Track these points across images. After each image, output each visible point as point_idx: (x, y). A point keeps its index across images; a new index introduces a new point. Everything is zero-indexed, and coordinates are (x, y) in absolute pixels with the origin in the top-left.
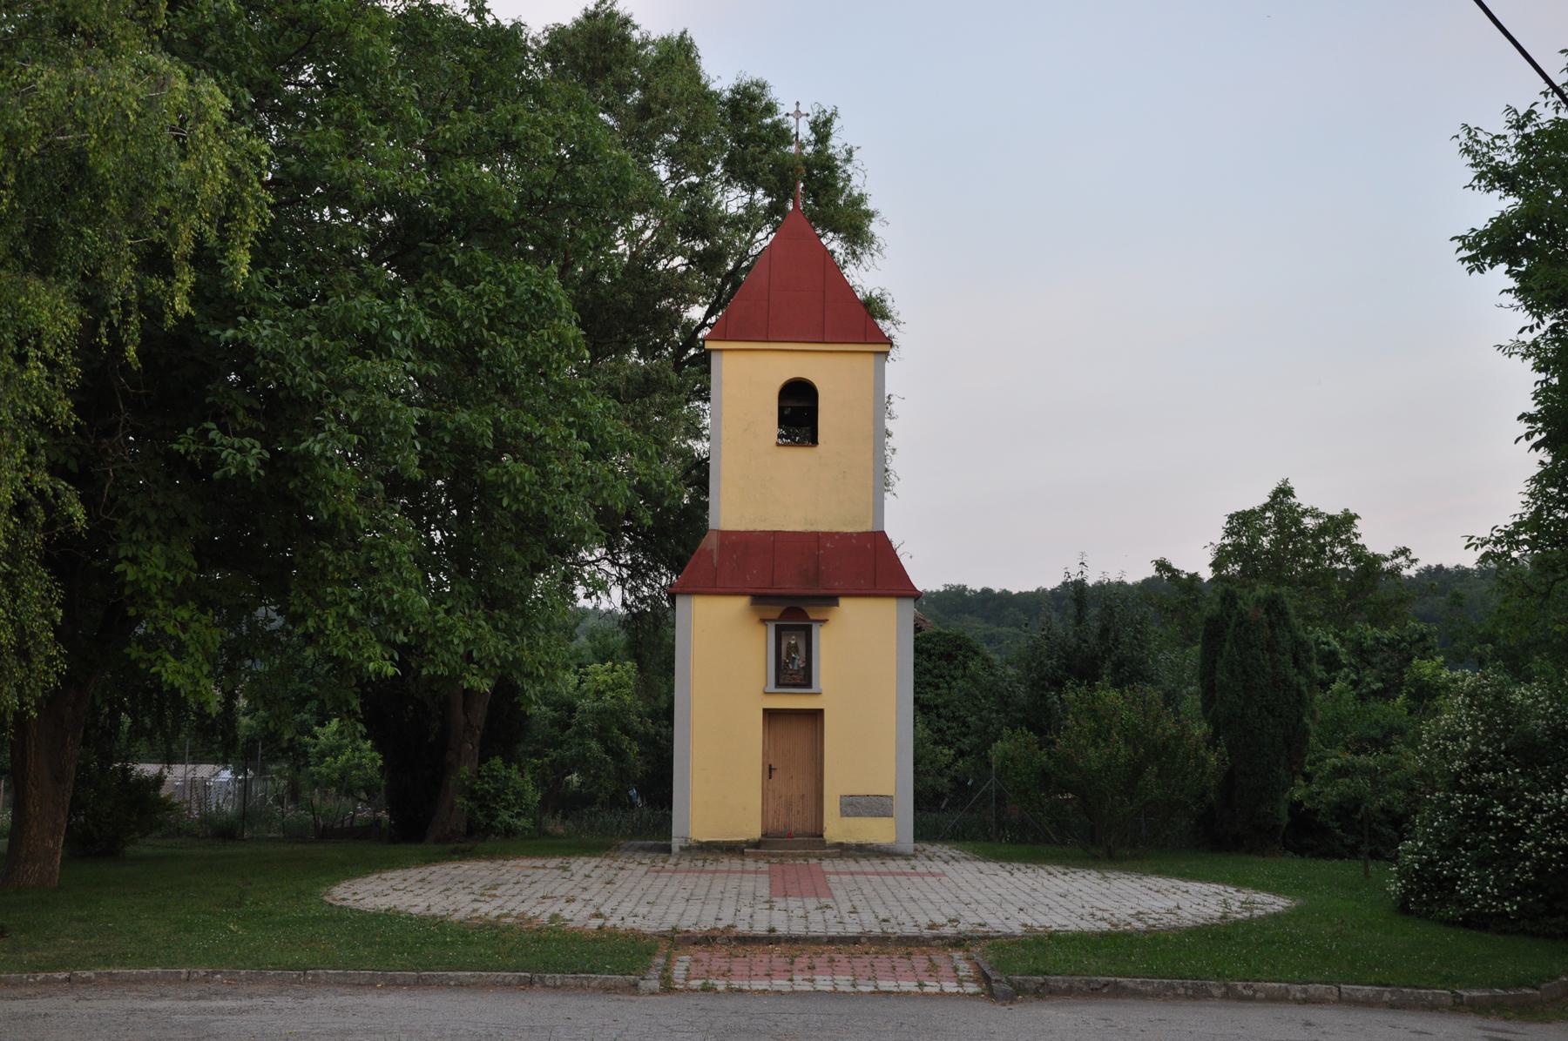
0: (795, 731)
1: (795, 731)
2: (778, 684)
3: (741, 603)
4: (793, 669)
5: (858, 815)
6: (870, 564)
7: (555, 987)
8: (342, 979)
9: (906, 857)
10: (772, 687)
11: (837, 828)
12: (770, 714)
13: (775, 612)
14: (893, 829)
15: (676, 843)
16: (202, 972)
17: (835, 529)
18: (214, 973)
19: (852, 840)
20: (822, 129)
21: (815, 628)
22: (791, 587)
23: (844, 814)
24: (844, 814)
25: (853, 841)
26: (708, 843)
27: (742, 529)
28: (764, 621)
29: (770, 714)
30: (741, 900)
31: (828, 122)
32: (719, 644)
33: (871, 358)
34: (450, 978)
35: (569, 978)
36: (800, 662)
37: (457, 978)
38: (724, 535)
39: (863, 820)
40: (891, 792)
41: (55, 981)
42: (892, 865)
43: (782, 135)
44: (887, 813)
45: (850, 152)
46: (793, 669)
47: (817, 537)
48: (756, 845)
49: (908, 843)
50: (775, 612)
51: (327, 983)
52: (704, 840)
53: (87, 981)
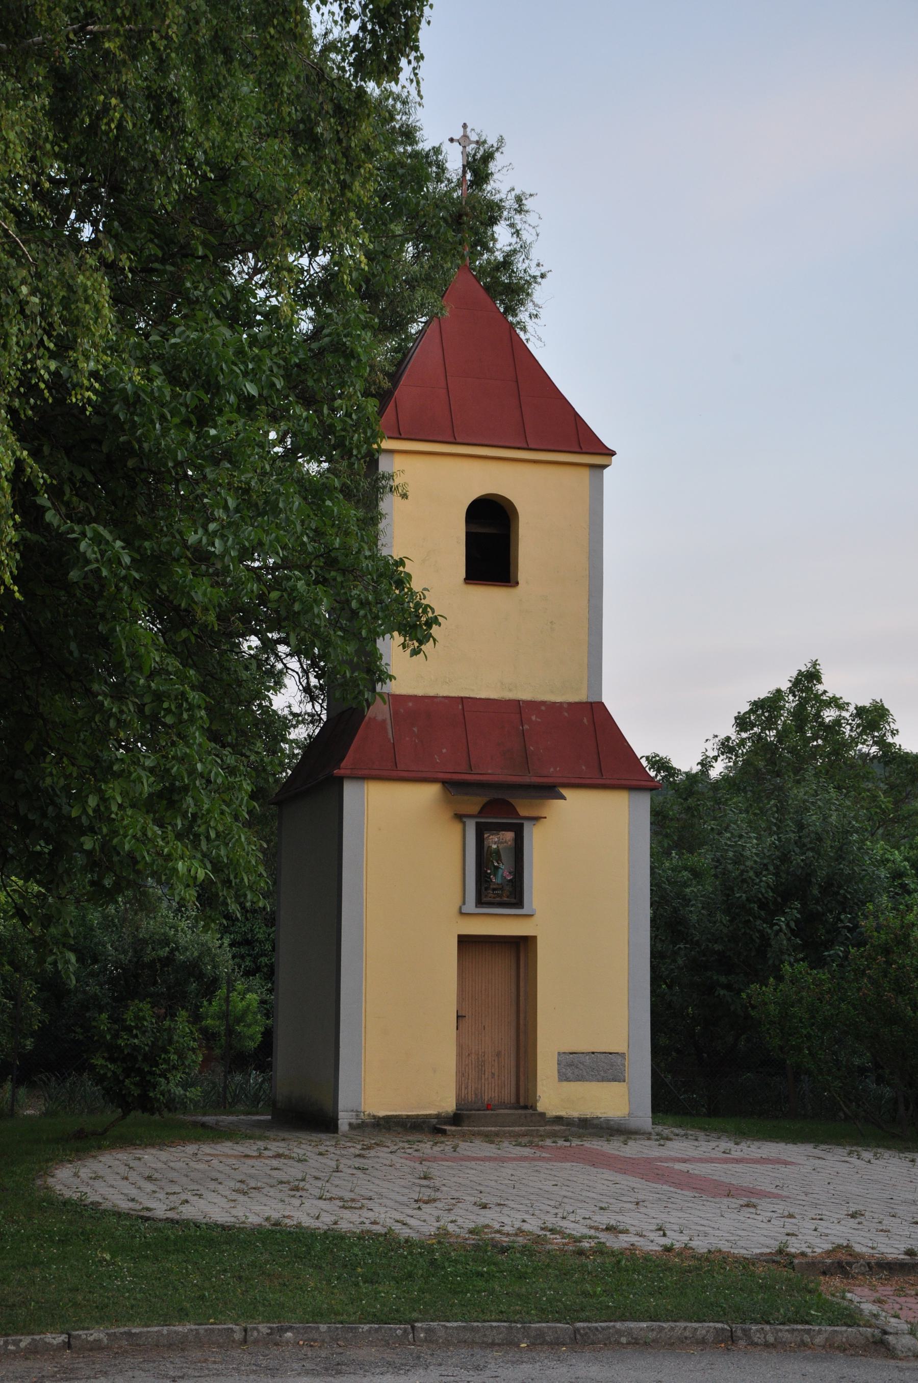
0: (501, 967)
1: (501, 967)
2: (480, 902)
3: (428, 793)
4: (499, 881)
5: (580, 1078)
6: (587, 746)
7: (767, 1345)
8: (468, 1336)
9: (648, 1136)
10: (471, 906)
11: (554, 1096)
12: (465, 942)
13: (473, 804)
14: (624, 1099)
15: (344, 1119)
16: (264, 1328)
17: (540, 697)
18: (282, 1330)
19: (574, 1113)
20: (479, 167)
21: (527, 826)
22: (494, 771)
23: (563, 1077)
24: (563, 1077)
25: (575, 1114)
26: (388, 1119)
27: (420, 692)
28: (460, 817)
29: (465, 942)
30: (385, 1199)
31: (488, 157)
32: (398, 841)
33: (585, 473)
34: (619, 1332)
35: (785, 1332)
36: (505, 871)
37: (629, 1332)
38: (399, 700)
39: (587, 1085)
40: (621, 1048)
41: (48, 1347)
42: (613, 1147)
43: (425, 165)
44: (617, 1078)
45: (519, 199)
46: (499, 881)
47: (518, 707)
48: (456, 1119)
49: (644, 1116)
50: (473, 804)
51: (447, 1343)
52: (382, 1113)
53: (96, 1347)
